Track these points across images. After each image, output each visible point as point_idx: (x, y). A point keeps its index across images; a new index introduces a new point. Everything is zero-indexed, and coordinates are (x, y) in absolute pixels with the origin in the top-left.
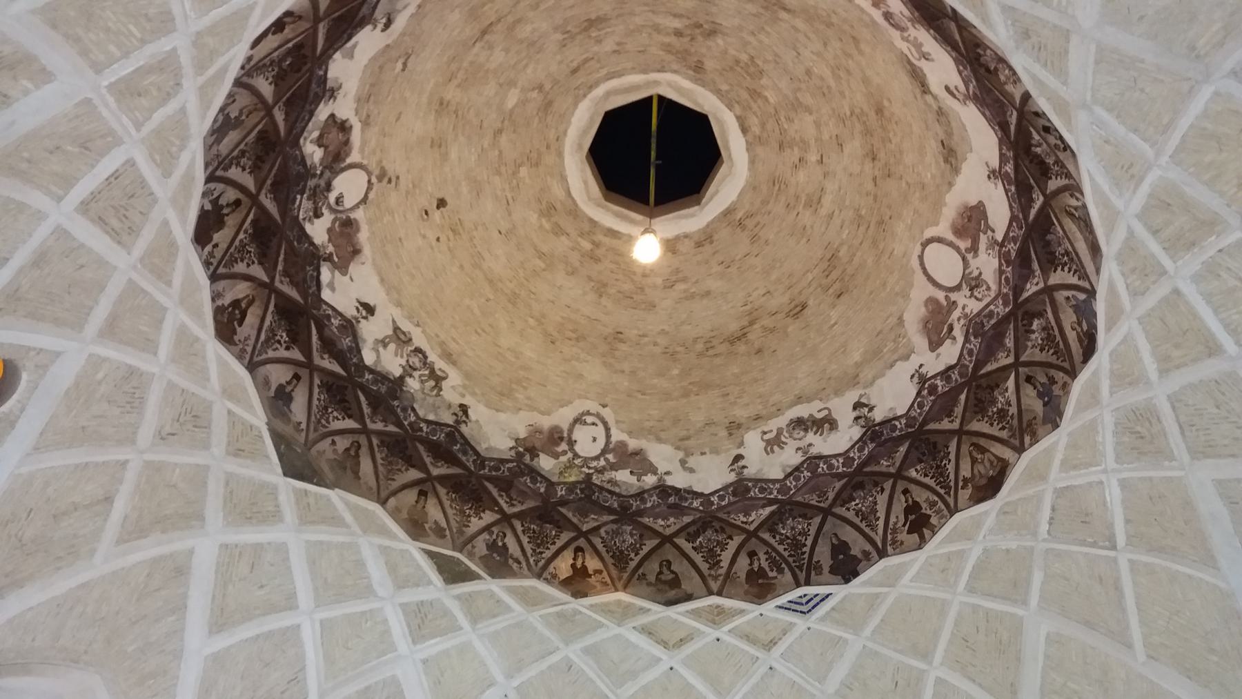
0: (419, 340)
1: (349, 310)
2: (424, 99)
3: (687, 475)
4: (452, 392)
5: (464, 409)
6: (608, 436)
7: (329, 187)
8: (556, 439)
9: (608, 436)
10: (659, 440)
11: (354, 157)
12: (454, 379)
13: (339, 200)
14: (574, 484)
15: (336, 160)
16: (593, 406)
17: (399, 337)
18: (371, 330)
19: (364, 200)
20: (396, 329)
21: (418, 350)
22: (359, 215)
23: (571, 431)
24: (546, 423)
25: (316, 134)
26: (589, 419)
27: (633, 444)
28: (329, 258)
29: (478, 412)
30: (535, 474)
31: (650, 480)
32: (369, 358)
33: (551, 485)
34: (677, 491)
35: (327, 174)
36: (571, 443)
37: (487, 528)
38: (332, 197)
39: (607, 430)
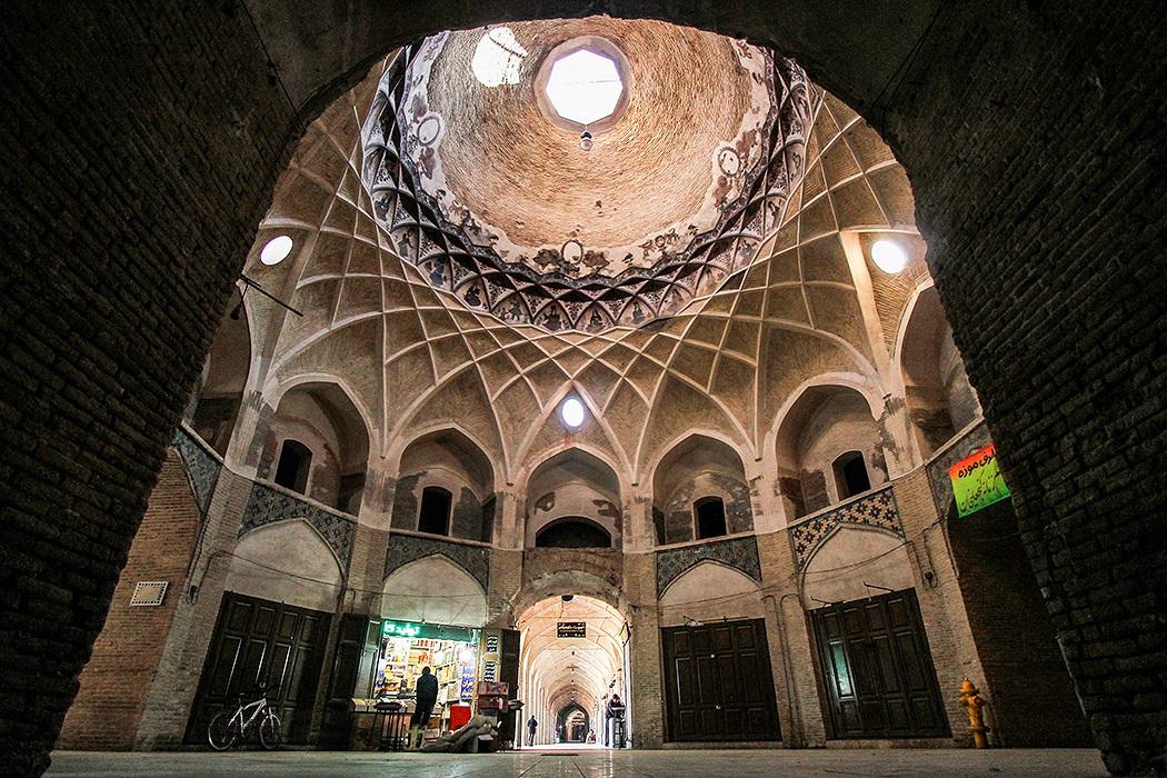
0: (652, 237)
1: (626, 266)
2: (544, 209)
3: (760, 113)
4: (680, 228)
5: (691, 227)
6: (732, 150)
7: (568, 263)
8: (723, 183)
9: (732, 150)
10: (741, 120)
11: (558, 248)
12: (676, 225)
13: (575, 259)
14: (745, 185)
15: (555, 257)
16: (717, 151)
17: (647, 247)
18: (638, 260)
19: (581, 245)
20: (643, 246)
21: (656, 239)
22: (586, 250)
23: (724, 171)
24: (715, 184)
25: (540, 267)
26: (722, 157)
27: (739, 137)
28: (599, 269)
29: (694, 220)
30: (731, 206)
31: (758, 137)
32: (648, 265)
33: (740, 200)
34: (766, 124)
35: (561, 263)
36: (728, 175)
37: (738, 249)
38: (573, 262)
39: (729, 149)
